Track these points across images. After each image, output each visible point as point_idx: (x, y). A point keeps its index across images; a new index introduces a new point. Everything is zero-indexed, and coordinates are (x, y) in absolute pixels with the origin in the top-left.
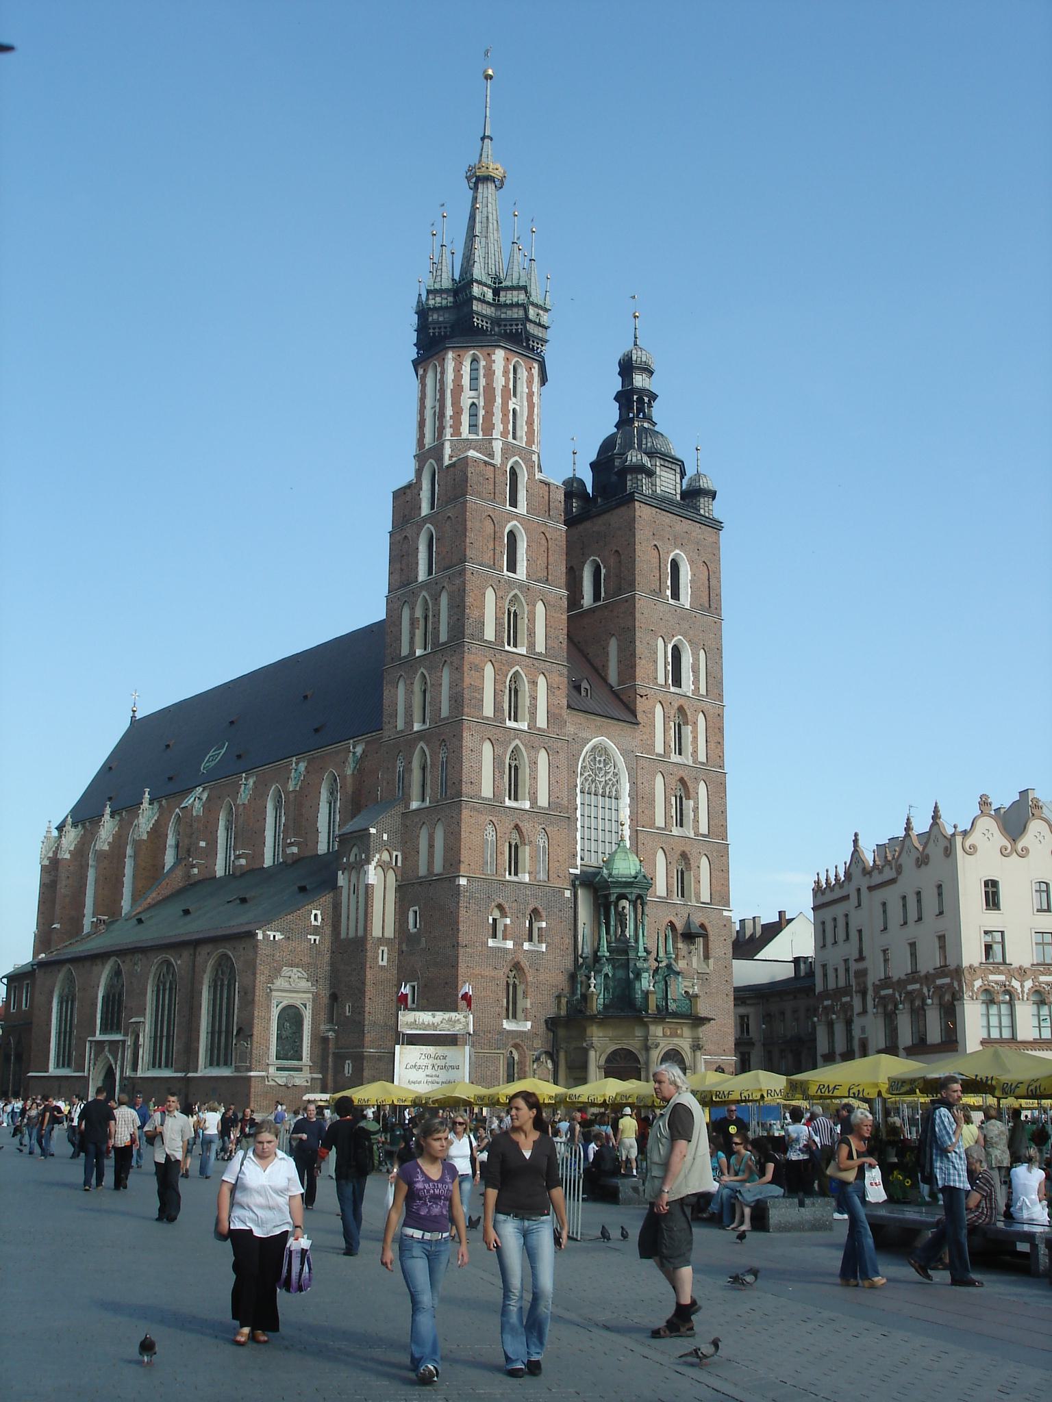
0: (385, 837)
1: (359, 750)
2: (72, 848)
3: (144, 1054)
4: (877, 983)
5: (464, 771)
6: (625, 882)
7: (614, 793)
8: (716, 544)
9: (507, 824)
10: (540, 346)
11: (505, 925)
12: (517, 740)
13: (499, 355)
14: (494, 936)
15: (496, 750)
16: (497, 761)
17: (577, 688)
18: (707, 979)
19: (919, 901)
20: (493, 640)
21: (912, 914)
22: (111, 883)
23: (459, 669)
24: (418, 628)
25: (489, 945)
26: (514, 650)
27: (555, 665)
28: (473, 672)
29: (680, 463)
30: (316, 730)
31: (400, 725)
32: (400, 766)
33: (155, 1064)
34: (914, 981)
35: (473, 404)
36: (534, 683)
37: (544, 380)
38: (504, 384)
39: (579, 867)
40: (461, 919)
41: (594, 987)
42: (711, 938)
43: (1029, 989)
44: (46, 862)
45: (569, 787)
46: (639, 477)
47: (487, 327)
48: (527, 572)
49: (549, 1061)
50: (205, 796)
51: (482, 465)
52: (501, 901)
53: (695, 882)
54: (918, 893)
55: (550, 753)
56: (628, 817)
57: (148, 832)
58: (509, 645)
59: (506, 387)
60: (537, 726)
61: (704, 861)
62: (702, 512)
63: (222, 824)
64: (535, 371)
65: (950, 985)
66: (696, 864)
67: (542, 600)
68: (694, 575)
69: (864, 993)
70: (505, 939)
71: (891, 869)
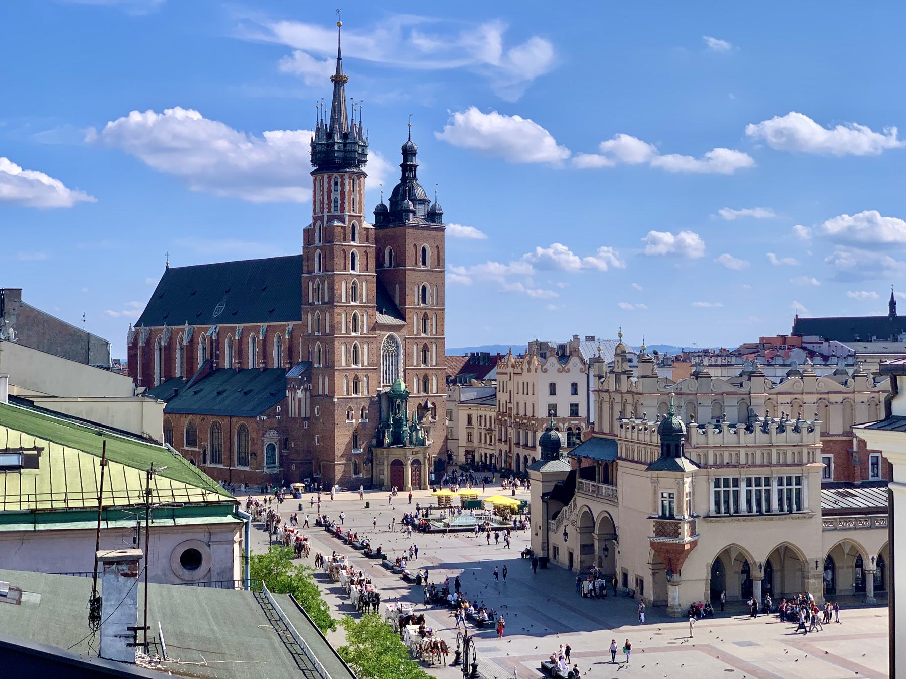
0: (305, 378)
1: (291, 327)
3: (209, 457)
8: (444, 236)
12: (356, 341)
13: (347, 176)
14: (348, 418)
21: (526, 393)
23: (332, 316)
30: (271, 312)
31: (310, 332)
32: (310, 348)
36: (363, 316)
42: (437, 408)
50: (217, 331)
59: (350, 190)
63: (227, 345)
69: (510, 417)
70: (352, 419)
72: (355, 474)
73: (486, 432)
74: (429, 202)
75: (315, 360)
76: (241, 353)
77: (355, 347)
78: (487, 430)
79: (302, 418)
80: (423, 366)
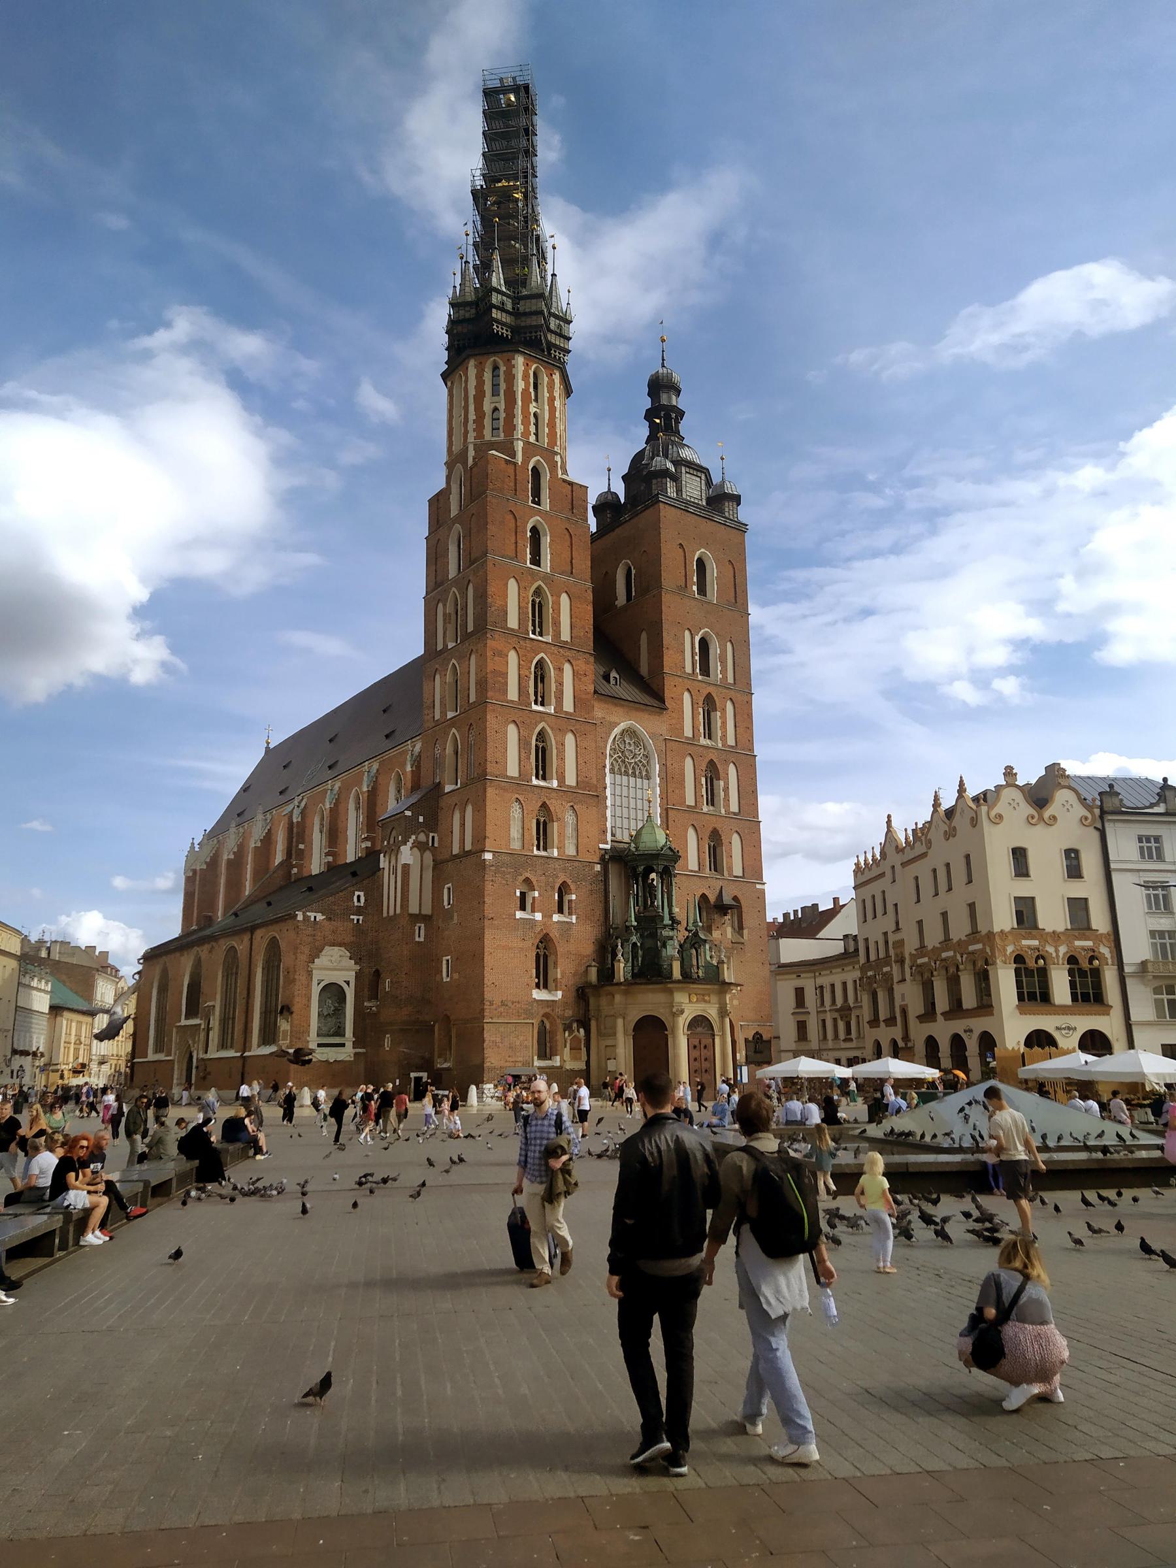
0: (421, 819)
2: (208, 860)
4: (914, 952)
5: (489, 751)
6: (651, 854)
7: (644, 773)
10: (562, 355)
11: (534, 898)
15: (521, 731)
16: (523, 743)
17: (606, 678)
19: (949, 872)
22: (234, 884)
23: (482, 656)
24: (450, 623)
25: (517, 917)
26: (540, 638)
27: (581, 653)
28: (496, 658)
33: (223, 1046)
34: (947, 950)
35: (496, 409)
36: (560, 670)
37: (568, 391)
39: (610, 842)
40: (486, 893)
41: (622, 955)
42: (744, 909)
43: (1064, 954)
44: (191, 874)
45: (598, 767)
46: (664, 480)
47: (507, 335)
49: (582, 1031)
51: (503, 462)
52: (528, 875)
53: (727, 857)
54: (948, 865)
55: (577, 735)
57: (261, 840)
58: (534, 633)
59: (526, 391)
61: (736, 839)
62: (727, 514)
64: (557, 377)
65: (983, 950)
67: (566, 592)
69: (901, 961)
70: (533, 911)
71: (922, 844)
72: (543, 1056)
73: (836, 1015)
74: (709, 482)
75: (448, 774)
76: (334, 835)
77: (541, 736)
78: (837, 1010)
79: (411, 915)
80: (705, 809)
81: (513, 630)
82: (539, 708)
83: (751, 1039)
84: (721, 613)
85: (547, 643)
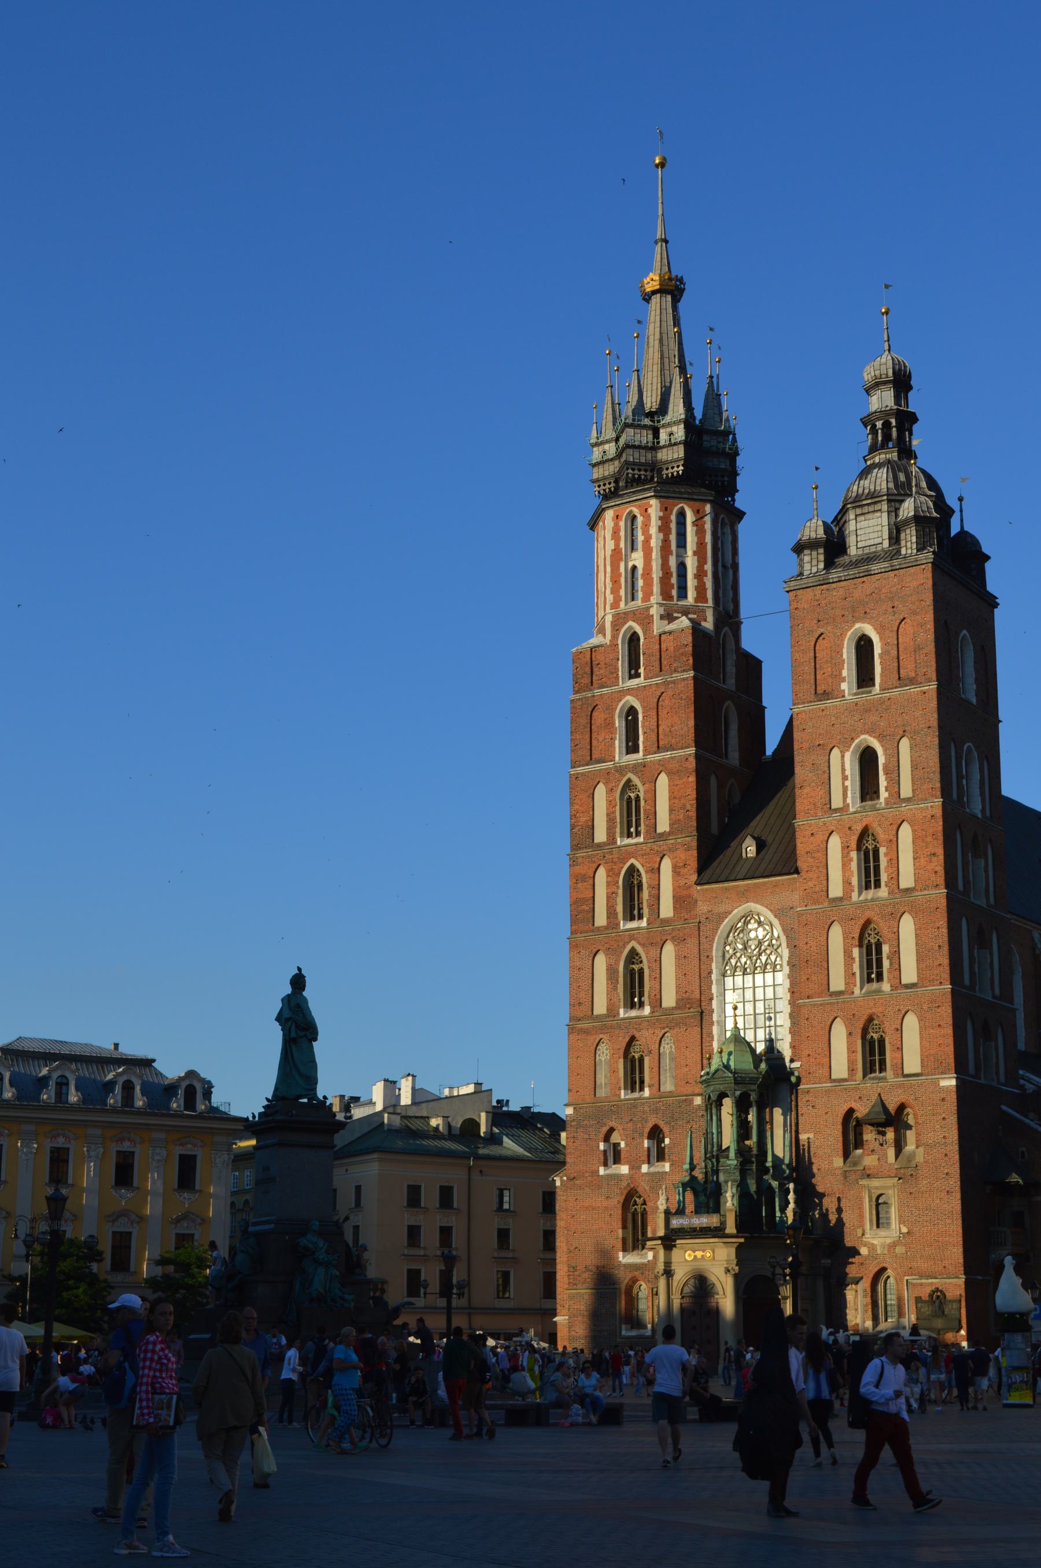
9: (621, 1038)
12: (633, 944)
18: (912, 1175)
20: (605, 840)
27: (679, 840)
28: (579, 885)
29: (885, 497)
38: (613, 548)
45: (703, 976)
47: (610, 489)
48: (645, 747)
52: (612, 1124)
56: (787, 990)
59: (616, 551)
60: (661, 916)
64: (654, 506)
66: (896, 1026)
68: (885, 644)
81: (600, 846)
82: (634, 924)
83: (925, 1297)
84: (888, 703)
85: (636, 844)
